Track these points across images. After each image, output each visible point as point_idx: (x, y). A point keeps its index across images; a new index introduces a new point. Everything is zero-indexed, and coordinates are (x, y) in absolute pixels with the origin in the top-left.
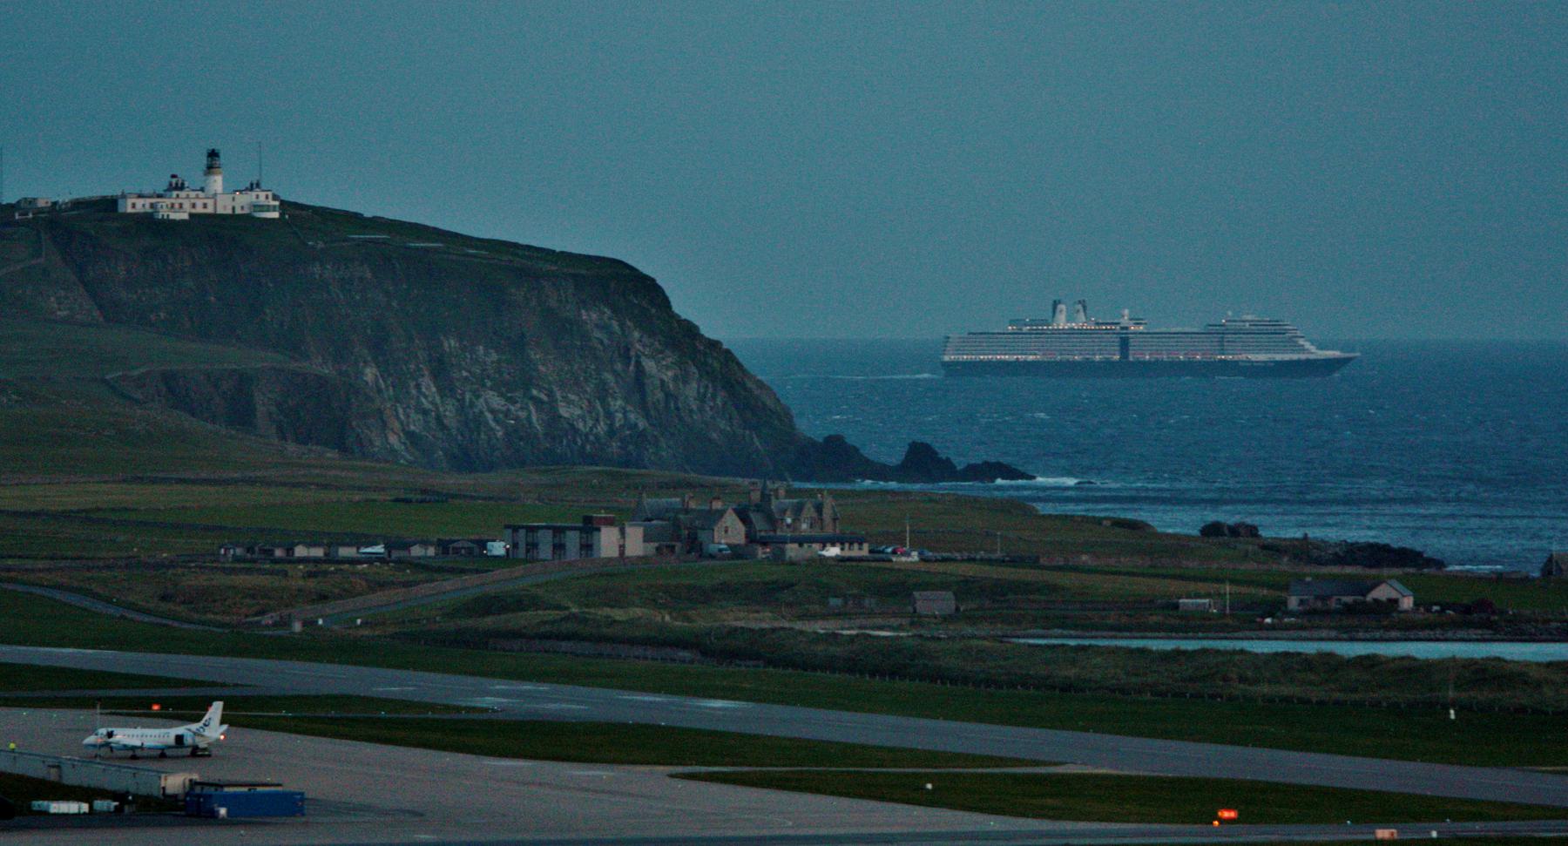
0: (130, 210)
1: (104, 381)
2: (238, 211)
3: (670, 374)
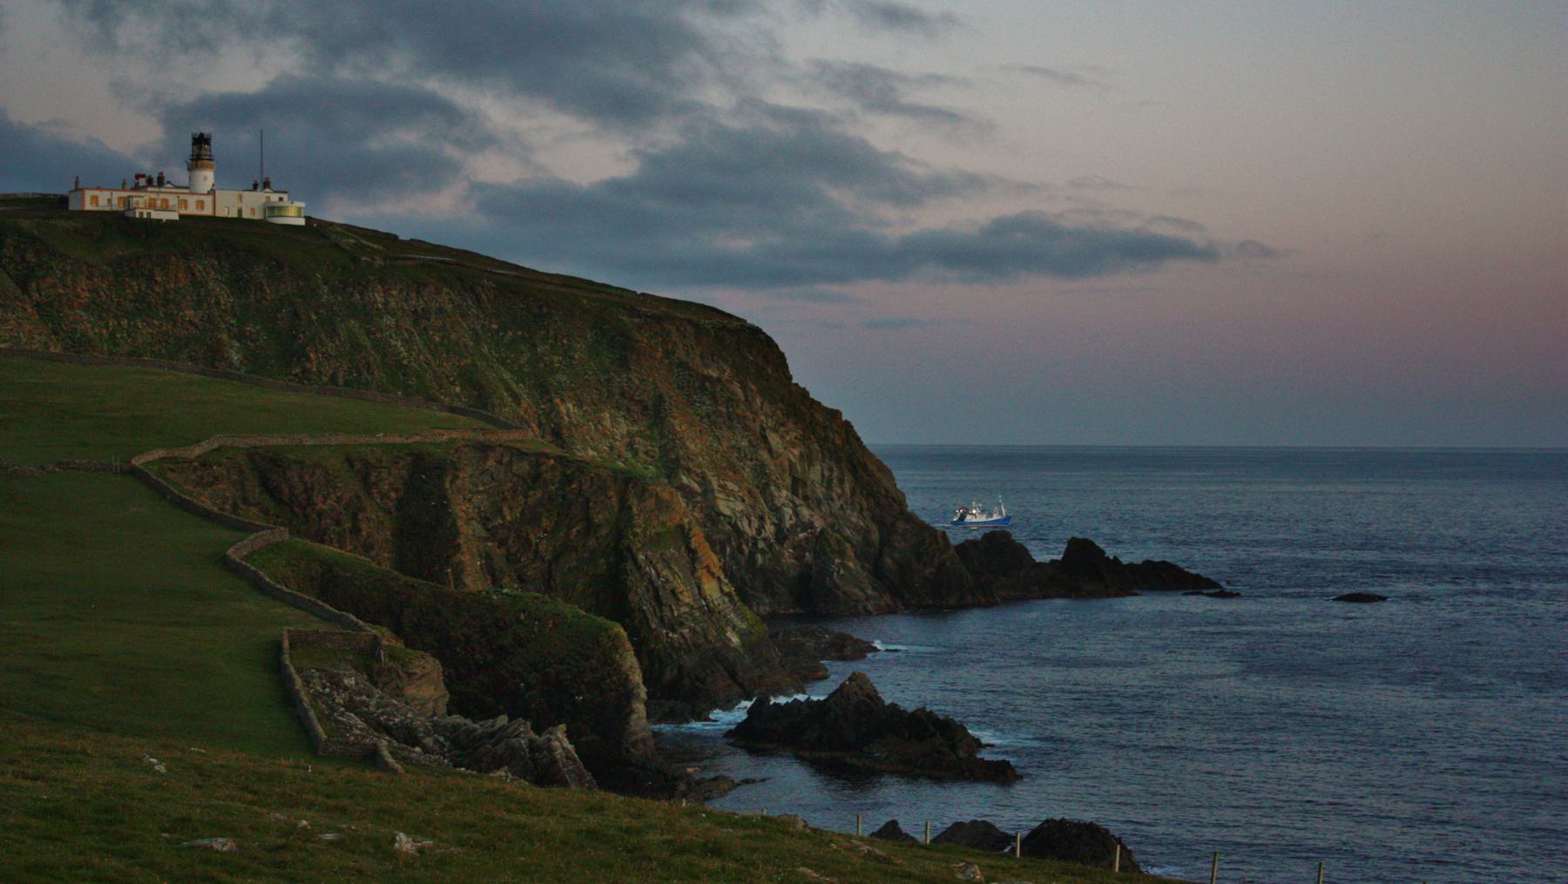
0: (88, 207)
1: (134, 472)
2: (246, 215)
3: (796, 452)
